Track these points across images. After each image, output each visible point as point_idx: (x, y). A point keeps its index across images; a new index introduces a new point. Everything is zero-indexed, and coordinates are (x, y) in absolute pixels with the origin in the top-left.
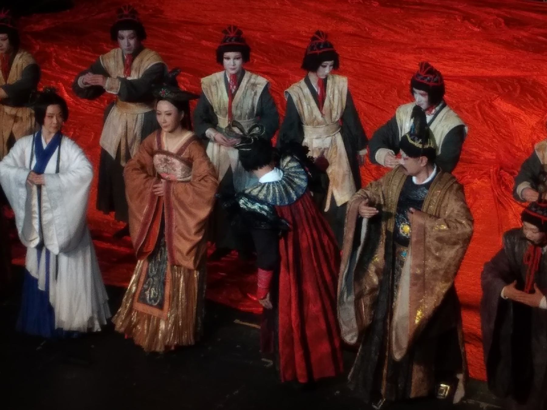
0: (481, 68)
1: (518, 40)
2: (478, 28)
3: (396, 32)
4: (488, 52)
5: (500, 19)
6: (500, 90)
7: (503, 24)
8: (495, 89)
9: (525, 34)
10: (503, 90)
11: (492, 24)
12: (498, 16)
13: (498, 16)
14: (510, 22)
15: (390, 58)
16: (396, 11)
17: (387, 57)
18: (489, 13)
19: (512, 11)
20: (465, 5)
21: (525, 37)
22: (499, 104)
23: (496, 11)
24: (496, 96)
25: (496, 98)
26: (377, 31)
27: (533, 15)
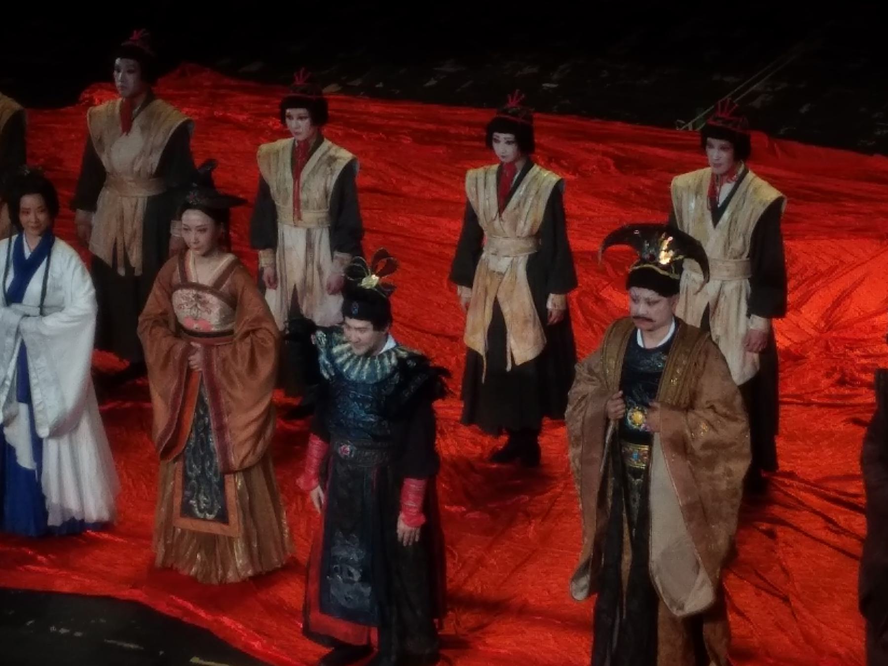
0: (581, 239)
1: (638, 192)
2: (574, 174)
3: (443, 185)
4: (590, 213)
5: (609, 160)
7: (613, 168)
9: (648, 182)
10: (617, 274)
12: (605, 154)
13: (605, 154)
14: (622, 164)
16: (441, 150)
17: (428, 226)
18: (590, 151)
19: (627, 147)
20: (551, 138)
21: (648, 187)
22: (611, 296)
23: (601, 147)
24: (605, 283)
25: (604, 287)
26: (409, 183)
27: (660, 152)
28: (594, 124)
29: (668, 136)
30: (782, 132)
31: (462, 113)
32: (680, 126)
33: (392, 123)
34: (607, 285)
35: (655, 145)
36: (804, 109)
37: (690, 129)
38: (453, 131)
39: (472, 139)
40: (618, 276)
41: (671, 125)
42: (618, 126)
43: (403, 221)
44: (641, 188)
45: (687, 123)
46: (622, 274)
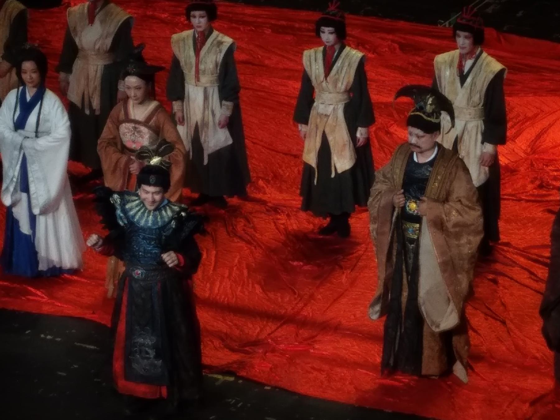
1: (414, 65)
4: (384, 79)
5: (396, 46)
6: (396, 116)
8: (391, 115)
9: (420, 59)
11: (387, 49)
12: (393, 41)
13: (393, 41)
15: (284, 86)
16: (289, 38)
18: (382, 39)
19: (407, 37)
23: (391, 37)
26: (270, 59)
27: (428, 40)
28: (386, 22)
29: (432, 30)
30: (505, 29)
31: (304, 14)
32: (441, 24)
33: (259, 20)
34: (394, 124)
35: (424, 36)
36: (520, 14)
37: (447, 26)
38: (297, 25)
39: (309, 30)
40: (401, 118)
41: (436, 24)
42: (401, 24)
43: (266, 83)
44: (416, 63)
45: (444, 22)
46: (402, 117)
